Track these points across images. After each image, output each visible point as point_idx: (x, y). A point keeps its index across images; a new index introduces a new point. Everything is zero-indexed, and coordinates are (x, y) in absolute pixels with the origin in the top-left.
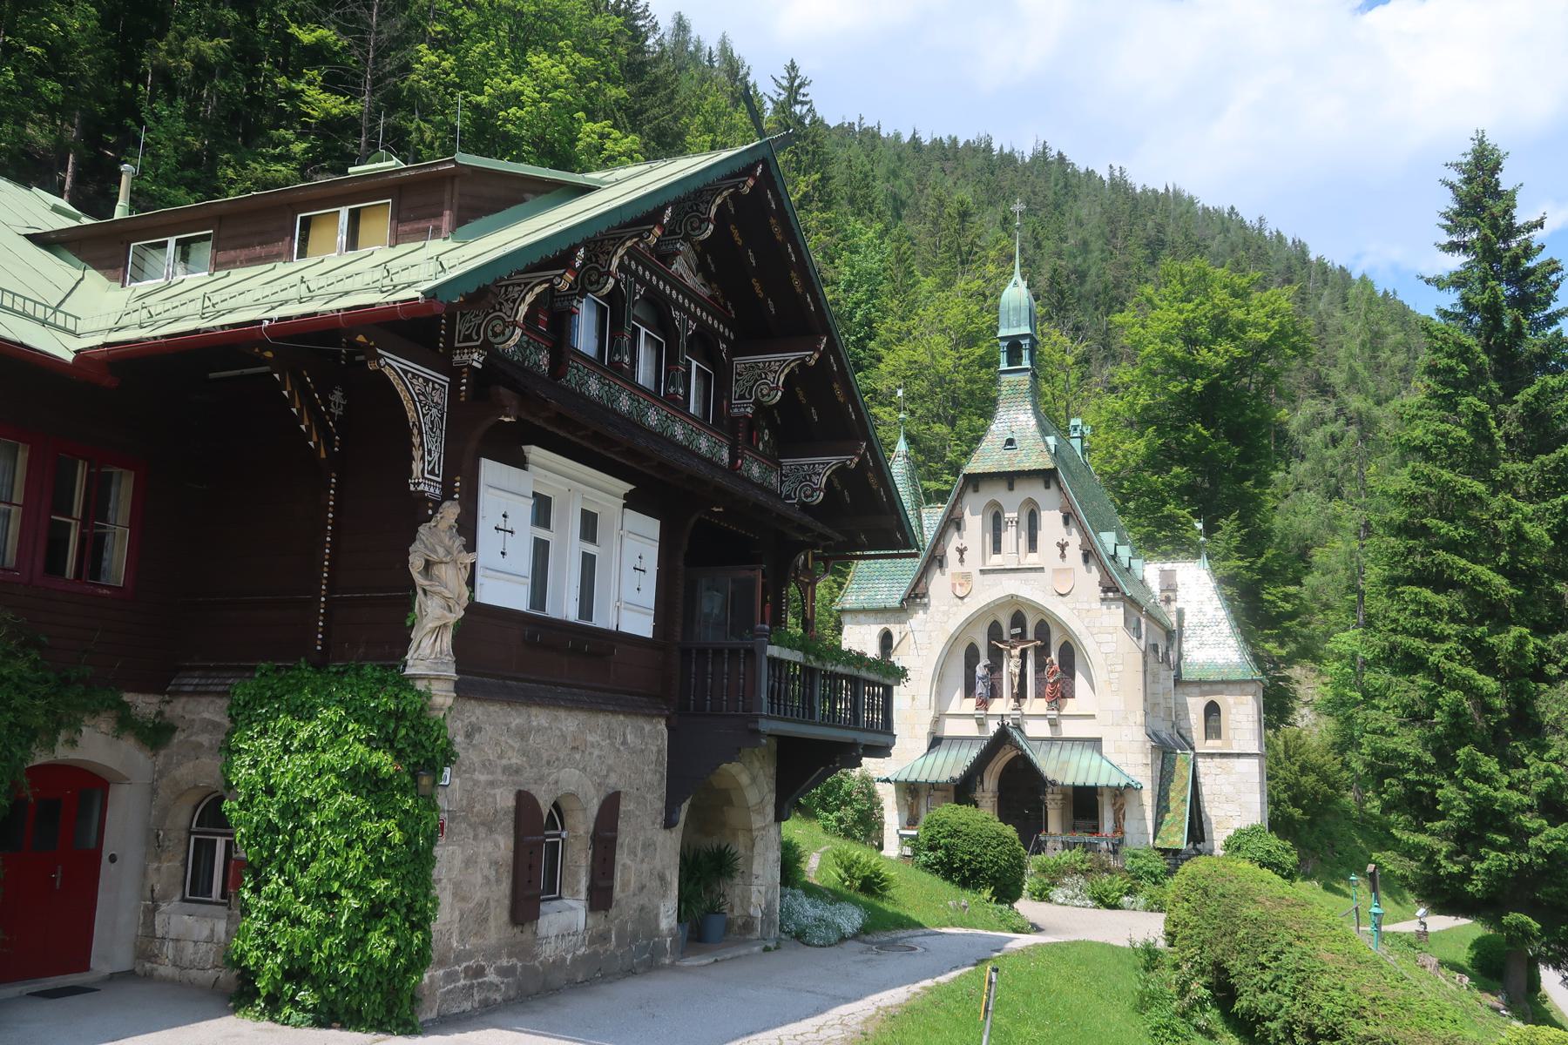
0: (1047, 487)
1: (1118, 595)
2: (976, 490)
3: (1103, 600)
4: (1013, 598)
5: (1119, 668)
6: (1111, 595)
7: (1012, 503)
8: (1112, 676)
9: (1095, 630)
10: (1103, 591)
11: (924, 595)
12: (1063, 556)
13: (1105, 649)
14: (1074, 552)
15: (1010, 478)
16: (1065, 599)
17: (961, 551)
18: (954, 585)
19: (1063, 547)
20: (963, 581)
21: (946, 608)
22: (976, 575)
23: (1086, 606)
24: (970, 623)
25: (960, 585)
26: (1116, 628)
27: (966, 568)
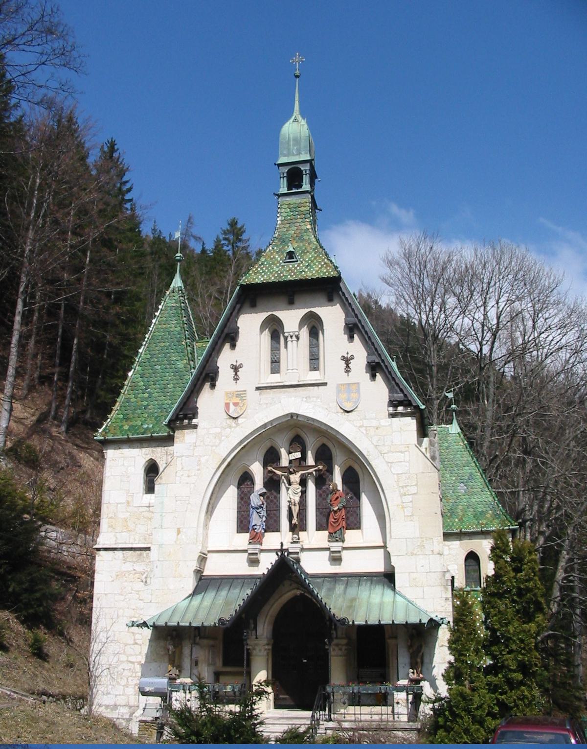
3: (393, 415)
5: (413, 490)
8: (407, 499)
9: (385, 449)
11: (195, 415)
12: (348, 370)
17: (236, 369)
18: (227, 405)
19: (347, 360)
20: (237, 400)
21: (218, 430)
23: (374, 423)
25: (236, 404)
27: (240, 386)
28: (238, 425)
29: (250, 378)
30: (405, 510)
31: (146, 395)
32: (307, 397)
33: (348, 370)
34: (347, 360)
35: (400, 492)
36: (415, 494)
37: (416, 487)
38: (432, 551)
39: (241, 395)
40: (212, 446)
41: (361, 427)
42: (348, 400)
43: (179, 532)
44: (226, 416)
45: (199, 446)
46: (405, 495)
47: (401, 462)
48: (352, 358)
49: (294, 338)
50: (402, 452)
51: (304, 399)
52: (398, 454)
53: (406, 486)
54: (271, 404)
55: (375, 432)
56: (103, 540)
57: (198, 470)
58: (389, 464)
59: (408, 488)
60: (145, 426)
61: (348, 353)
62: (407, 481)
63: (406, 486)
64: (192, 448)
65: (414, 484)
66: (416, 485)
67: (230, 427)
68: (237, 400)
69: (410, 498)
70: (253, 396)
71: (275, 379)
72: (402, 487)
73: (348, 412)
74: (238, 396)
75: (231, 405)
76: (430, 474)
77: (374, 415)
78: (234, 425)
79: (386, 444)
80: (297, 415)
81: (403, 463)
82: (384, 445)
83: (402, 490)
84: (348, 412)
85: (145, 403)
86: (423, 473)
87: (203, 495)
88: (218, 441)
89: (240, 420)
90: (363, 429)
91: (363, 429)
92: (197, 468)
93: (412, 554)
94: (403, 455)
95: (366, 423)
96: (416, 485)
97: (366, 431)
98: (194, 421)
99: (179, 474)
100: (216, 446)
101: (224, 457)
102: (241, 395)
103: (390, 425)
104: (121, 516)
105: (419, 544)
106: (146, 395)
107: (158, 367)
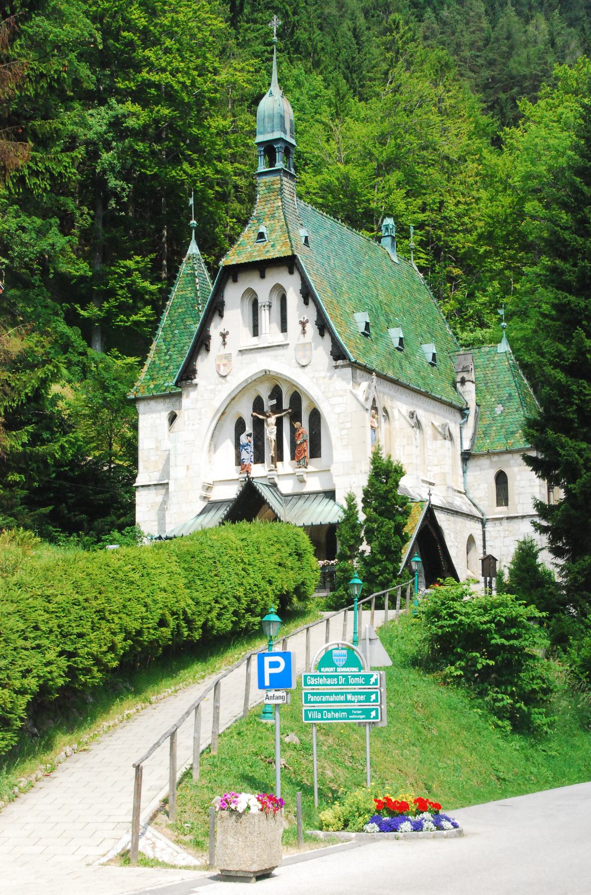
0: (291, 272)
1: (346, 362)
2: (235, 281)
3: (336, 367)
4: (266, 375)
5: (349, 425)
6: (340, 362)
7: (263, 288)
12: (304, 332)
13: (338, 410)
15: (261, 267)
16: (307, 369)
17: (224, 336)
18: (219, 366)
19: (303, 324)
20: (225, 361)
21: (213, 387)
24: (233, 399)
25: (224, 365)
28: (226, 381)
31: (168, 357)
32: (276, 356)
33: (304, 332)
34: (303, 324)
39: (228, 357)
41: (313, 378)
42: (304, 357)
48: (307, 321)
49: (267, 308)
50: (341, 396)
56: (139, 481)
60: (166, 385)
66: (351, 421)
67: (221, 384)
70: (236, 359)
71: (254, 342)
73: (304, 366)
74: (226, 358)
75: (222, 368)
85: (167, 364)
89: (228, 378)
96: (351, 421)
98: (195, 381)
99: (187, 423)
101: (218, 407)
102: (228, 357)
104: (153, 458)
106: (168, 357)
107: (177, 332)
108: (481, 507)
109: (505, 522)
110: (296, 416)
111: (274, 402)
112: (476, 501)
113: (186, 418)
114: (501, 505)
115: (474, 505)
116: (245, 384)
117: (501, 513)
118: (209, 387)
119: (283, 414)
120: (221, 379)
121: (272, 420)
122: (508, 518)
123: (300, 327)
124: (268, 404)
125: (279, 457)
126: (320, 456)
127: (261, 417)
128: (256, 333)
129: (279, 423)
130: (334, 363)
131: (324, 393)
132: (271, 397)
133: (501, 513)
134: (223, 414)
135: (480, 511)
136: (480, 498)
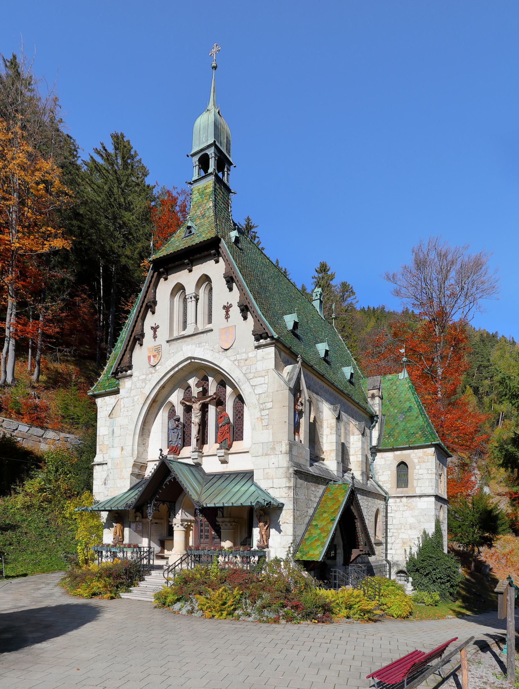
3: (258, 347)
5: (269, 405)
6: (262, 341)
9: (251, 376)
10: (257, 340)
11: (130, 367)
12: (227, 317)
13: (258, 390)
14: (235, 311)
18: (149, 357)
19: (227, 308)
21: (144, 377)
22: (165, 346)
23: (244, 356)
25: (154, 356)
26: (267, 371)
28: (156, 371)
29: (163, 334)
30: (263, 421)
33: (227, 317)
34: (227, 308)
35: (260, 407)
36: (270, 408)
37: (271, 403)
38: (281, 451)
40: (141, 388)
41: (235, 360)
43: (122, 449)
44: (149, 366)
45: (133, 389)
46: (264, 410)
47: (262, 384)
48: (231, 306)
51: (198, 345)
52: (260, 378)
53: (264, 403)
54: (176, 352)
55: (244, 363)
57: (133, 406)
58: (253, 387)
59: (266, 404)
61: (228, 303)
62: (265, 399)
63: (264, 403)
64: (129, 391)
65: (271, 400)
66: (272, 401)
67: (151, 373)
68: (155, 353)
69: (267, 412)
72: (262, 404)
73: (226, 350)
75: (152, 358)
76: (282, 392)
77: (244, 349)
78: (154, 371)
79: (252, 371)
80: (194, 358)
81: (263, 385)
82: (250, 372)
83: (261, 406)
84: (226, 350)
86: (277, 391)
87: (135, 423)
88: (144, 384)
89: (158, 367)
90: (236, 363)
91: (236, 363)
92: (132, 404)
93: (266, 455)
94: (263, 378)
95: (239, 357)
96: (272, 401)
97: (238, 363)
99: (122, 411)
100: (143, 388)
103: (256, 356)
105: (271, 447)
108: (385, 488)
109: (404, 500)
110: (220, 403)
111: (201, 389)
112: (381, 483)
113: (122, 406)
114: (402, 487)
115: (379, 486)
116: (172, 373)
117: (402, 493)
118: (141, 378)
119: (209, 399)
120: (152, 370)
121: (196, 406)
122: (407, 497)
123: (224, 312)
124: (195, 391)
125: (203, 440)
126: (242, 440)
127: (188, 403)
128: (185, 327)
129: (204, 409)
130: (256, 343)
131: (245, 374)
132: (197, 385)
133: (402, 493)
134: (154, 401)
135: (384, 491)
136: (384, 481)
